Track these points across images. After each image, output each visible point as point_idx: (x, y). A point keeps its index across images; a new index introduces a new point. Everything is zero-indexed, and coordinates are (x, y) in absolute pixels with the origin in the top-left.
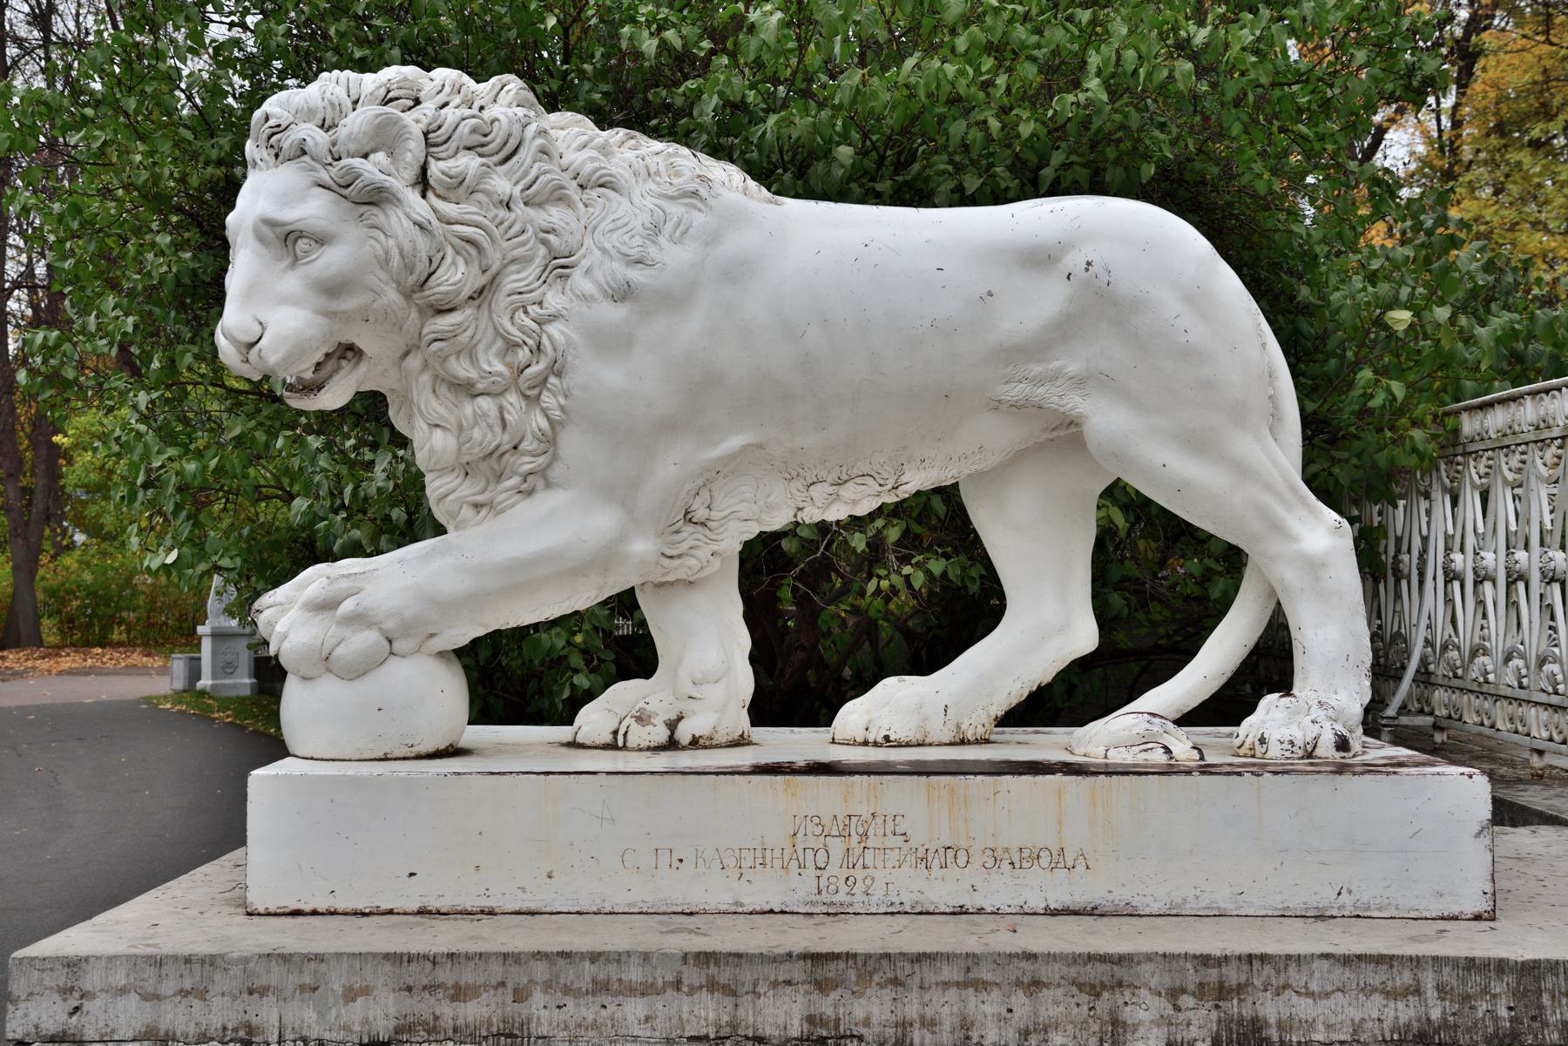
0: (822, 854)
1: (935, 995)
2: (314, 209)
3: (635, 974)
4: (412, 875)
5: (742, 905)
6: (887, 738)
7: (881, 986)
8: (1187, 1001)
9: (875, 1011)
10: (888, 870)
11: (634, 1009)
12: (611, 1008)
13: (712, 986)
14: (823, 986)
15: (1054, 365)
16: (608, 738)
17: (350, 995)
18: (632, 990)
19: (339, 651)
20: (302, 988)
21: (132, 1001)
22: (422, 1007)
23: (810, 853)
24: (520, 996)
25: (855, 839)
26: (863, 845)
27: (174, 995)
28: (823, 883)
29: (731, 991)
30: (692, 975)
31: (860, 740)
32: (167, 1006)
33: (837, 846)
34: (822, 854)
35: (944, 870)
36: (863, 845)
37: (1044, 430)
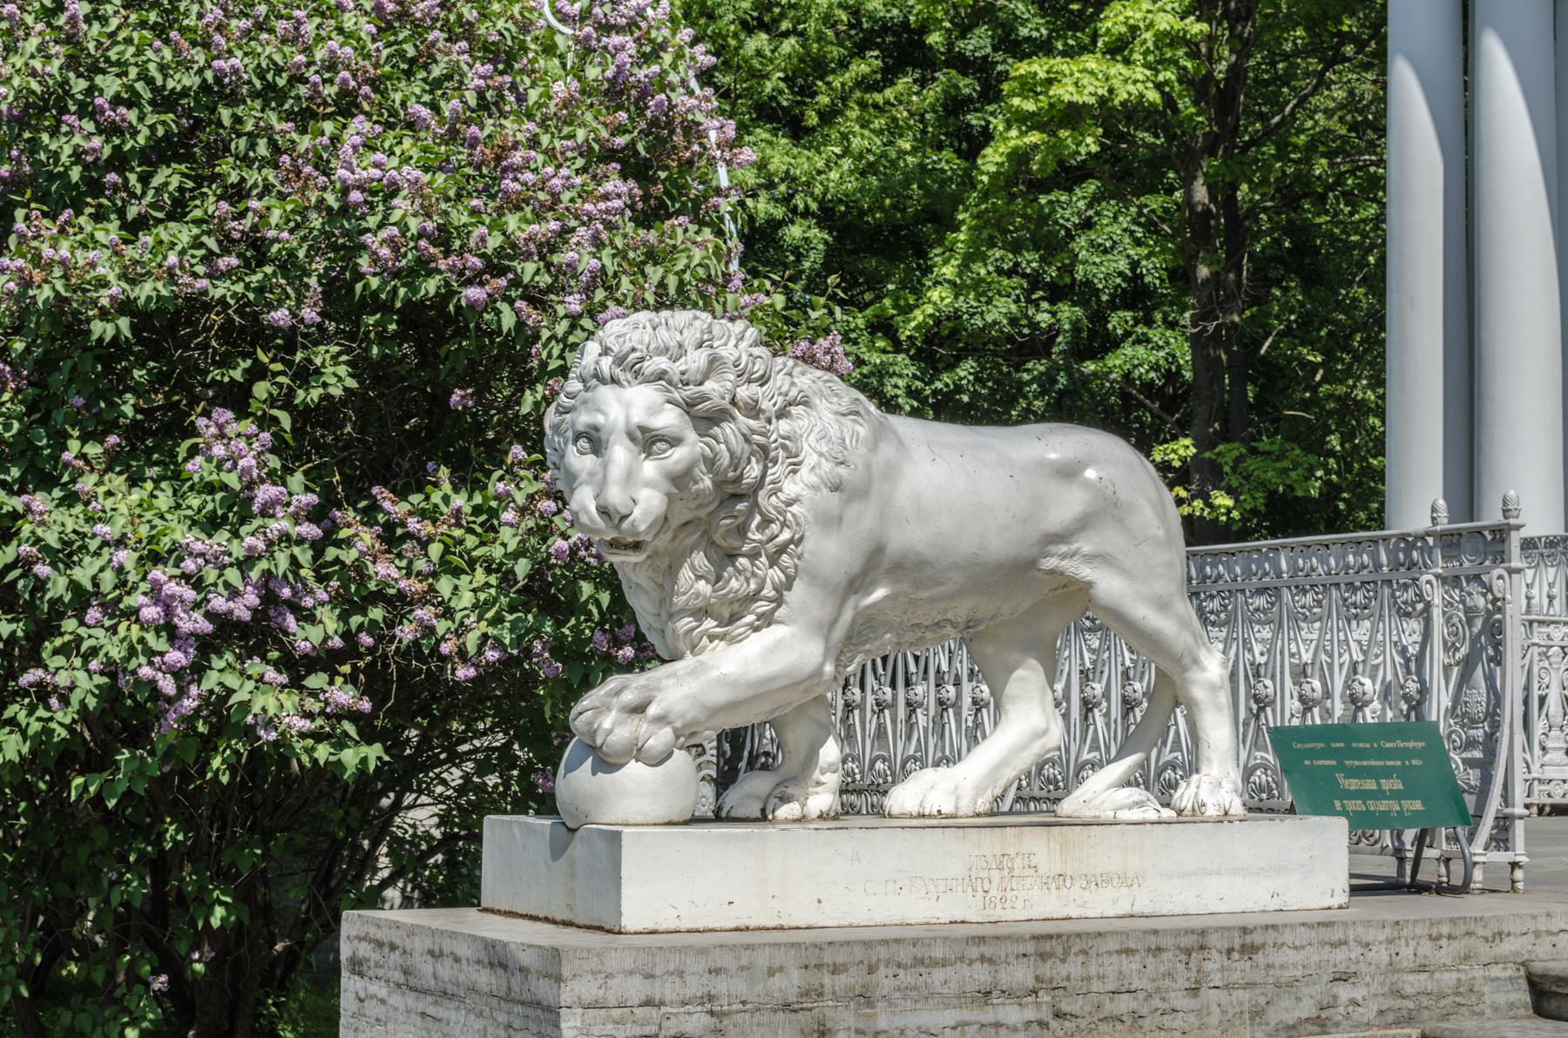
1: (1106, 960)
2: (669, 419)
3: (938, 953)
7: (1076, 955)
8: (1236, 956)
9: (1073, 971)
11: (939, 975)
13: (982, 959)
14: (1043, 956)
15: (1074, 546)
17: (771, 972)
18: (935, 963)
19: (651, 742)
20: (742, 968)
21: (637, 979)
22: (813, 978)
24: (871, 970)
29: (991, 961)
30: (974, 952)
32: (658, 982)
33: (995, 873)
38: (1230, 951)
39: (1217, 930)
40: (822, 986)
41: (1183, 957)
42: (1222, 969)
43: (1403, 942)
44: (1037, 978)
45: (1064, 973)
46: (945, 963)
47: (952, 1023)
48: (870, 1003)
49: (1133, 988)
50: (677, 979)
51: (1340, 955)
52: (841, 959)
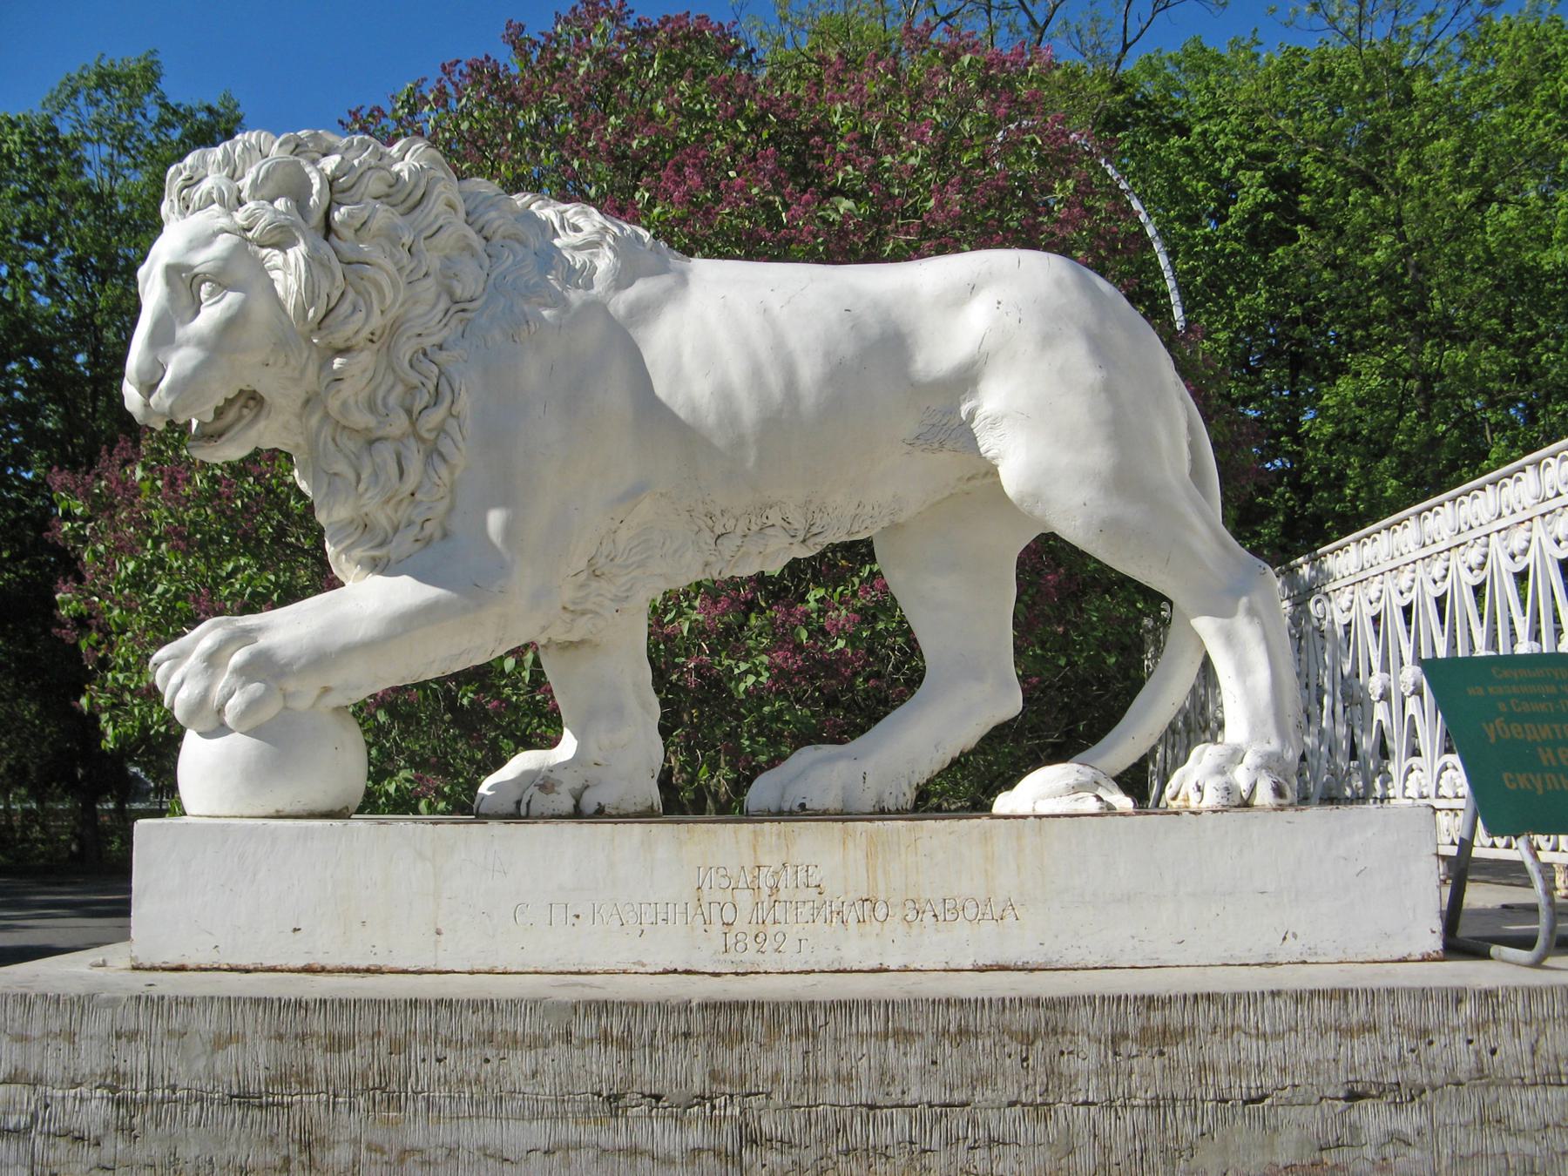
0: (728, 908)
3: (524, 1026)
4: (295, 930)
5: (644, 965)
6: (802, 806)
10: (800, 926)
11: (520, 1063)
12: (494, 1062)
13: (605, 1038)
16: (511, 808)
17: (220, 1042)
18: (515, 1042)
23: (715, 909)
24: (397, 1047)
25: (766, 891)
26: (773, 898)
27: (43, 1036)
28: (731, 940)
29: (625, 1043)
30: (585, 1028)
31: (773, 809)
34: (728, 908)
35: (861, 924)
36: (773, 898)
37: (960, 479)
38: (1117, 1039)
39: (1089, 1000)
40: (309, 1069)
41: (1014, 1047)
42: (1102, 1071)
43: (1504, 1029)
44: (714, 1076)
45: (767, 1068)
46: (537, 1043)
47: (543, 1143)
48: (393, 1101)
49: (908, 1100)
50: (64, 1046)
51: (1362, 1050)
52: (343, 1027)
